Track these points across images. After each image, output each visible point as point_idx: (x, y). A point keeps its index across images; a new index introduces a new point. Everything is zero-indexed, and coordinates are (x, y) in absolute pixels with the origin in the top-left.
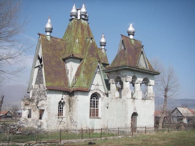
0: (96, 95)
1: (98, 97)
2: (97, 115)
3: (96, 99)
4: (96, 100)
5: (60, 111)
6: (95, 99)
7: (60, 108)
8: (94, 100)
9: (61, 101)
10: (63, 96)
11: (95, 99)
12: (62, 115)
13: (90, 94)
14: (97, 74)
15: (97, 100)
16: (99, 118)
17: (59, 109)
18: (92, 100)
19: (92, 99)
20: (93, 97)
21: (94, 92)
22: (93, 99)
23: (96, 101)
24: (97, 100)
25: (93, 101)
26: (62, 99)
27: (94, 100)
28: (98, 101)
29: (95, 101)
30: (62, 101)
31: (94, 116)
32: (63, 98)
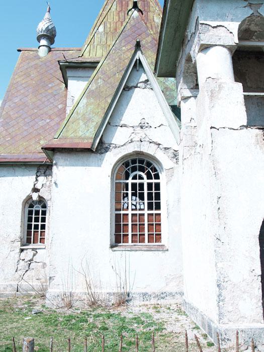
0: (149, 164)
1: (155, 170)
2: (158, 237)
3: (149, 177)
4: (146, 181)
5: (36, 227)
6: (141, 178)
7: (37, 220)
8: (138, 181)
9: (30, 197)
10: (37, 180)
11: (141, 178)
12: (42, 241)
13: (111, 158)
14: (136, 89)
15: (154, 181)
16: (163, 249)
17: (30, 220)
18: (130, 181)
19: (127, 178)
20: (134, 169)
21: (130, 149)
22: (135, 178)
23: (150, 185)
24: (154, 181)
25: (134, 185)
26: (36, 190)
27: (138, 181)
28: (158, 186)
29: (142, 185)
30: (35, 197)
31: (142, 241)
32: (38, 186)
